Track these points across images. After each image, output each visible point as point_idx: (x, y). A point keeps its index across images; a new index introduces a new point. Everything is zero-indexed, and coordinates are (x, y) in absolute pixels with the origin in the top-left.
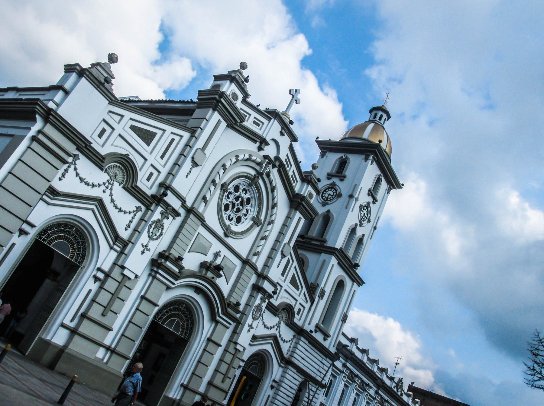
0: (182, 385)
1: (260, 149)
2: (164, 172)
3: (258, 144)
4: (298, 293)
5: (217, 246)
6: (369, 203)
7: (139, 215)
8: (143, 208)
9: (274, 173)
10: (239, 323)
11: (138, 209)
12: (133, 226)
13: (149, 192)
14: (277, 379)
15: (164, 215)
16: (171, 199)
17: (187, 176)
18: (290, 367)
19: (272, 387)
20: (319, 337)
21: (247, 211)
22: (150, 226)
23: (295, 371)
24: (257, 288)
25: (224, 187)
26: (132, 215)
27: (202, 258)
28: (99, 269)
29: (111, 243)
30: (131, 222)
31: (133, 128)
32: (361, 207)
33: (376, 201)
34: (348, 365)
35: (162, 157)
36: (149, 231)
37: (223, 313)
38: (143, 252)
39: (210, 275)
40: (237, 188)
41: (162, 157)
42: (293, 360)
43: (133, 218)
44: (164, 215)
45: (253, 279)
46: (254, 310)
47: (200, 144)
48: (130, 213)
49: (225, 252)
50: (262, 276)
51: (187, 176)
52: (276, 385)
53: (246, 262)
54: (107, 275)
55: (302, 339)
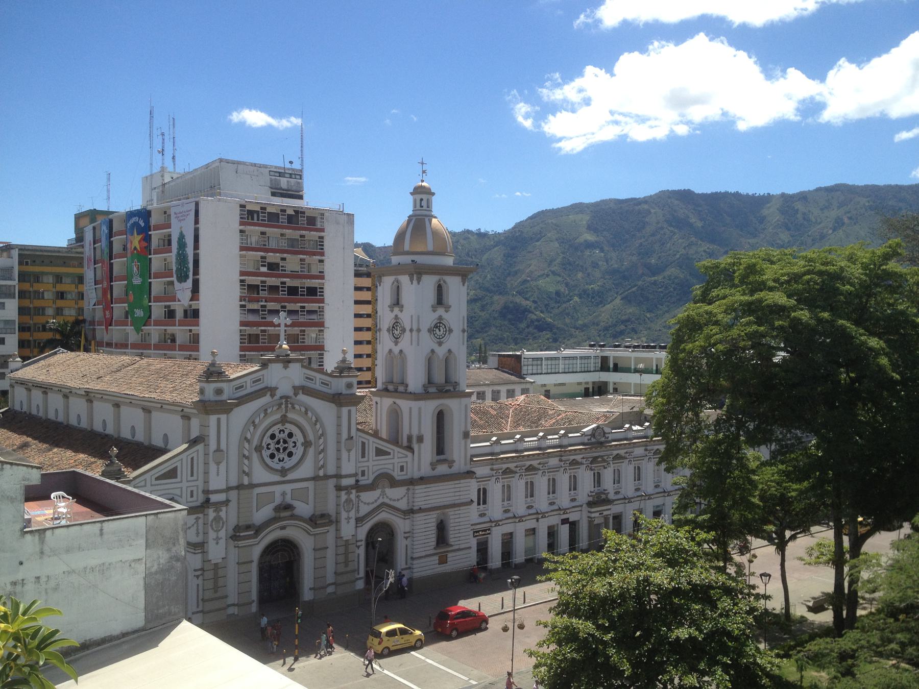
0: (311, 589)
1: (272, 396)
2: (200, 483)
3: (269, 393)
4: (391, 456)
5: (278, 489)
6: (440, 318)
7: (201, 521)
8: (201, 515)
9: (302, 397)
10: (338, 522)
11: (197, 519)
12: (201, 531)
13: (198, 504)
14: (407, 530)
15: (217, 510)
16: (214, 498)
17: (218, 475)
19: (406, 538)
20: (442, 469)
21: (295, 443)
22: (212, 526)
24: (339, 488)
25: (259, 449)
26: (195, 525)
27: (272, 506)
28: (195, 570)
29: (192, 551)
30: (197, 530)
31: (157, 479)
32: (430, 331)
33: (450, 307)
34: (495, 467)
35: (192, 475)
36: (213, 529)
38: (217, 543)
39: (284, 514)
40: (273, 437)
41: (192, 475)
43: (198, 526)
44: (217, 510)
45: (332, 482)
46: (344, 506)
47: (213, 446)
48: (193, 525)
49: (288, 488)
50: (338, 476)
51: (218, 475)
52: (409, 535)
53: (315, 478)
54: (202, 569)
55: (416, 487)
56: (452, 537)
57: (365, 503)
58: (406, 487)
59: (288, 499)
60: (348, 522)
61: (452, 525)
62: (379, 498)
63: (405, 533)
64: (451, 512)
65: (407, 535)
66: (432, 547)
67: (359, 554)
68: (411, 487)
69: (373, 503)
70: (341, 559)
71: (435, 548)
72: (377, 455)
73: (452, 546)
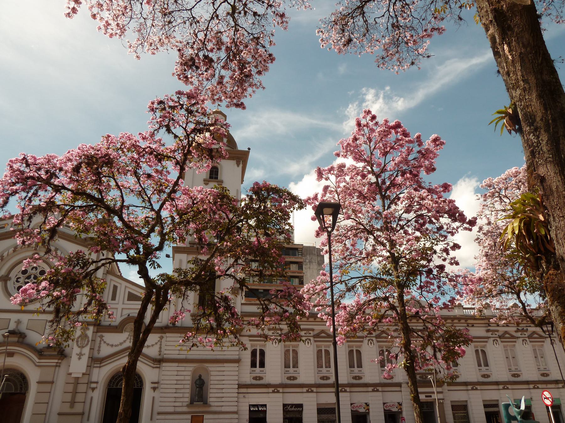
5: (14, 317)
18: (164, 364)
23: (176, 364)
37: (39, 359)
42: (165, 356)
55: (168, 335)
56: (213, 396)
57: (108, 344)
58: (159, 335)
59: (23, 328)
60: (80, 359)
61: (212, 382)
62: (125, 341)
63: (152, 383)
64: (212, 368)
65: (156, 385)
66: (185, 404)
67: (92, 398)
68: (163, 335)
69: (116, 346)
70: (69, 397)
71: (187, 406)
72: (128, 300)
73: (210, 406)
